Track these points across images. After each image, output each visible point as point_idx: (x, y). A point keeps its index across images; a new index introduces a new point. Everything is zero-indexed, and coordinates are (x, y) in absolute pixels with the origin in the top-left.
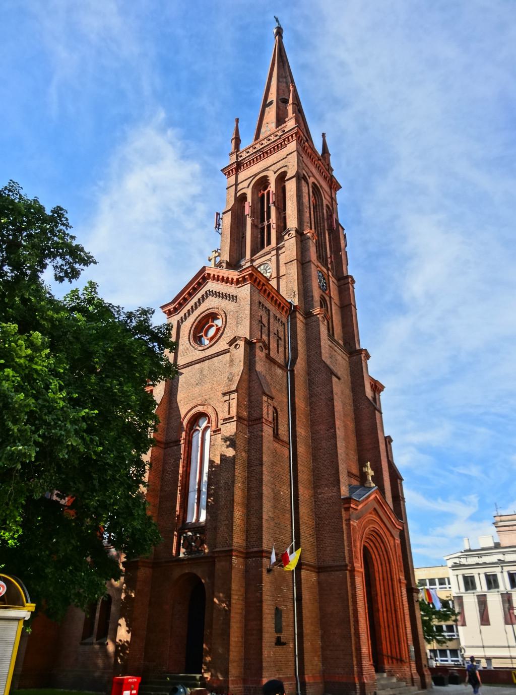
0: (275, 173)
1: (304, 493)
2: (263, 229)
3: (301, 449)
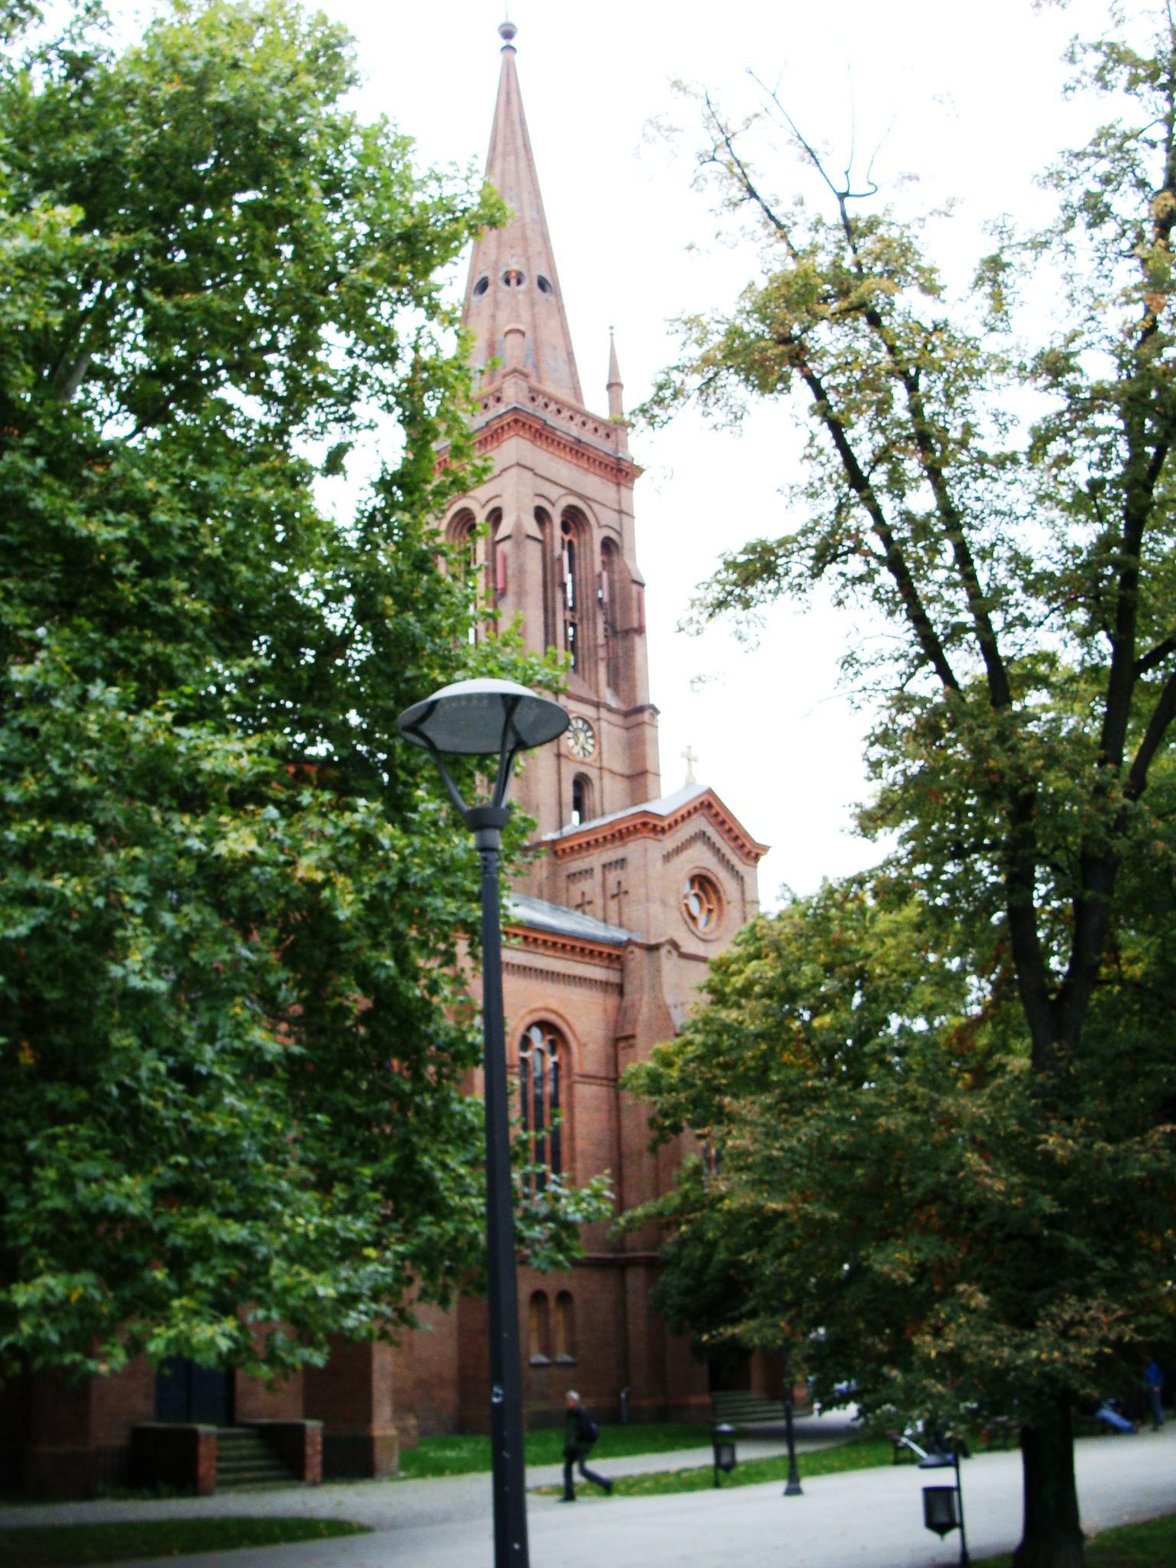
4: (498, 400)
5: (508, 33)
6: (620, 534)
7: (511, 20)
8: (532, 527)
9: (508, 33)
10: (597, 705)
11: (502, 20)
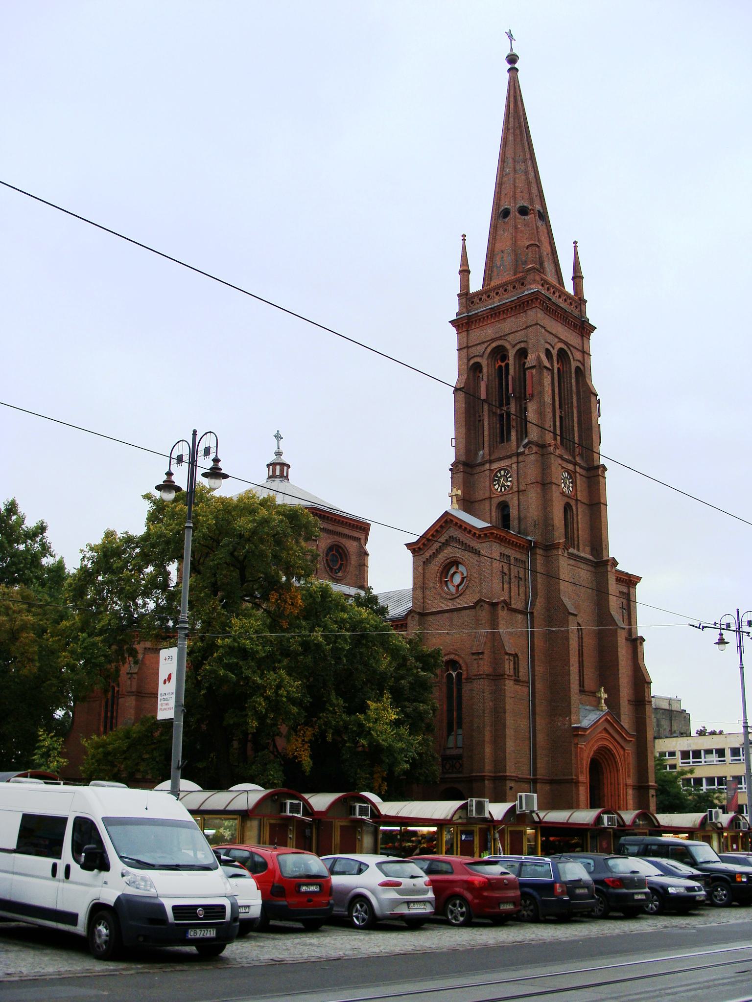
0: (514, 347)
1: (541, 723)
2: (501, 415)
3: (539, 686)
4: (523, 284)
5: (512, 59)
6: (583, 365)
8: (546, 363)
9: (512, 59)
10: (575, 464)
11: (508, 52)
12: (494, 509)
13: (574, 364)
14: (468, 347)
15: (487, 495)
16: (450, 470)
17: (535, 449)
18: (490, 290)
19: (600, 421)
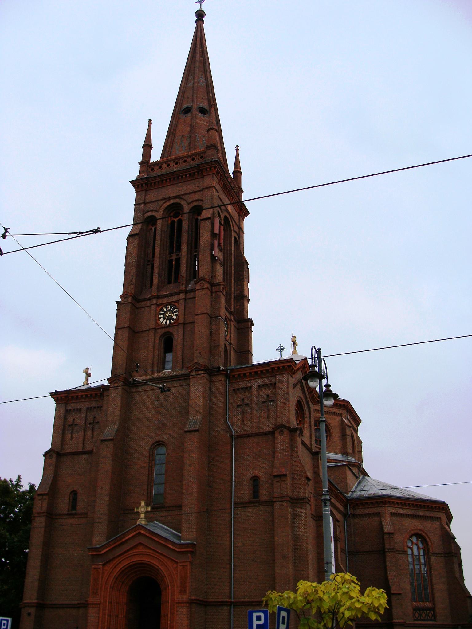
0: (189, 204)
2: (170, 261)
5: (200, 15)
6: (239, 239)
7: (203, 9)
9: (200, 15)
11: (199, 9)
12: (157, 338)
13: (234, 235)
14: (145, 203)
15: (152, 326)
16: (117, 302)
17: (206, 285)
18: (170, 161)
19: (250, 285)
